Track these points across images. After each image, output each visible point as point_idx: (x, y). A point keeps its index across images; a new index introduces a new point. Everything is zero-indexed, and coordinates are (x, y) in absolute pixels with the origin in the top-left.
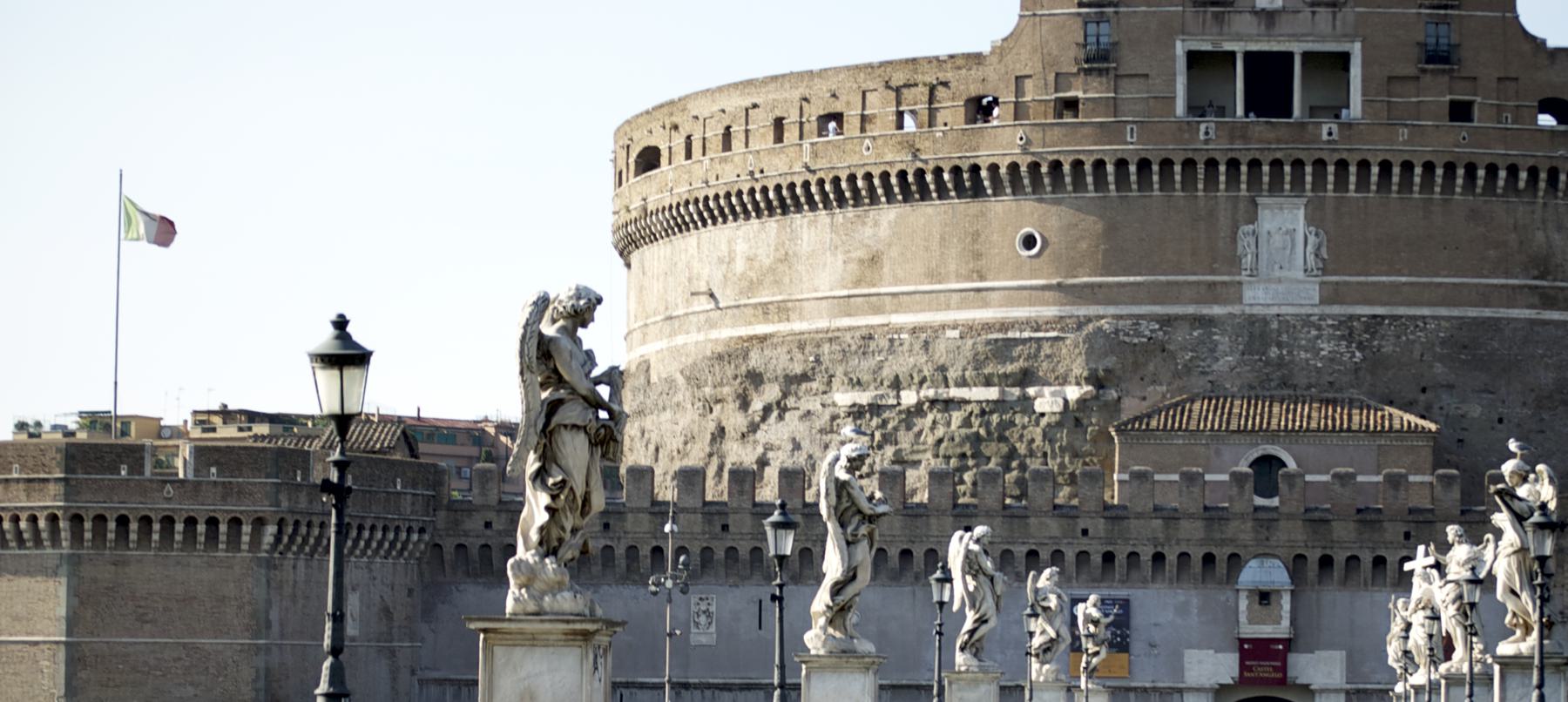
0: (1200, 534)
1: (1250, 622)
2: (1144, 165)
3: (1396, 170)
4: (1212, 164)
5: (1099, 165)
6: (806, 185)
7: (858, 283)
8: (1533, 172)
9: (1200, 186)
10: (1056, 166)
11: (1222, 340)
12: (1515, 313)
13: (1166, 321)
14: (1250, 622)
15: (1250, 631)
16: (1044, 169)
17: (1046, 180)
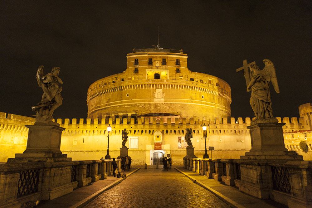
0: (148, 127)
1: (156, 140)
2: (142, 85)
3: (173, 86)
4: (150, 85)
5: (136, 85)
6: (102, 91)
7: (107, 102)
8: (190, 87)
9: (149, 87)
10: (131, 86)
11: (152, 107)
12: (188, 103)
13: (145, 104)
14: (156, 140)
15: (156, 142)
16: (130, 86)
17: (130, 87)
